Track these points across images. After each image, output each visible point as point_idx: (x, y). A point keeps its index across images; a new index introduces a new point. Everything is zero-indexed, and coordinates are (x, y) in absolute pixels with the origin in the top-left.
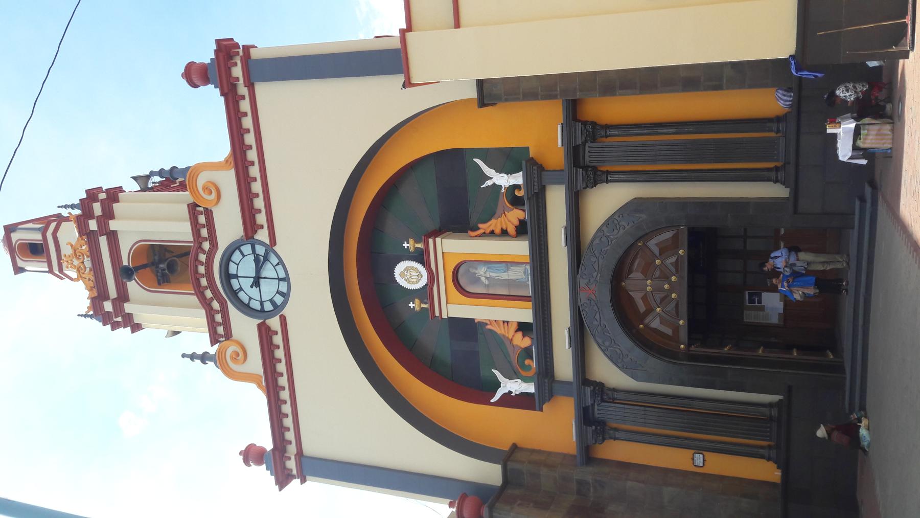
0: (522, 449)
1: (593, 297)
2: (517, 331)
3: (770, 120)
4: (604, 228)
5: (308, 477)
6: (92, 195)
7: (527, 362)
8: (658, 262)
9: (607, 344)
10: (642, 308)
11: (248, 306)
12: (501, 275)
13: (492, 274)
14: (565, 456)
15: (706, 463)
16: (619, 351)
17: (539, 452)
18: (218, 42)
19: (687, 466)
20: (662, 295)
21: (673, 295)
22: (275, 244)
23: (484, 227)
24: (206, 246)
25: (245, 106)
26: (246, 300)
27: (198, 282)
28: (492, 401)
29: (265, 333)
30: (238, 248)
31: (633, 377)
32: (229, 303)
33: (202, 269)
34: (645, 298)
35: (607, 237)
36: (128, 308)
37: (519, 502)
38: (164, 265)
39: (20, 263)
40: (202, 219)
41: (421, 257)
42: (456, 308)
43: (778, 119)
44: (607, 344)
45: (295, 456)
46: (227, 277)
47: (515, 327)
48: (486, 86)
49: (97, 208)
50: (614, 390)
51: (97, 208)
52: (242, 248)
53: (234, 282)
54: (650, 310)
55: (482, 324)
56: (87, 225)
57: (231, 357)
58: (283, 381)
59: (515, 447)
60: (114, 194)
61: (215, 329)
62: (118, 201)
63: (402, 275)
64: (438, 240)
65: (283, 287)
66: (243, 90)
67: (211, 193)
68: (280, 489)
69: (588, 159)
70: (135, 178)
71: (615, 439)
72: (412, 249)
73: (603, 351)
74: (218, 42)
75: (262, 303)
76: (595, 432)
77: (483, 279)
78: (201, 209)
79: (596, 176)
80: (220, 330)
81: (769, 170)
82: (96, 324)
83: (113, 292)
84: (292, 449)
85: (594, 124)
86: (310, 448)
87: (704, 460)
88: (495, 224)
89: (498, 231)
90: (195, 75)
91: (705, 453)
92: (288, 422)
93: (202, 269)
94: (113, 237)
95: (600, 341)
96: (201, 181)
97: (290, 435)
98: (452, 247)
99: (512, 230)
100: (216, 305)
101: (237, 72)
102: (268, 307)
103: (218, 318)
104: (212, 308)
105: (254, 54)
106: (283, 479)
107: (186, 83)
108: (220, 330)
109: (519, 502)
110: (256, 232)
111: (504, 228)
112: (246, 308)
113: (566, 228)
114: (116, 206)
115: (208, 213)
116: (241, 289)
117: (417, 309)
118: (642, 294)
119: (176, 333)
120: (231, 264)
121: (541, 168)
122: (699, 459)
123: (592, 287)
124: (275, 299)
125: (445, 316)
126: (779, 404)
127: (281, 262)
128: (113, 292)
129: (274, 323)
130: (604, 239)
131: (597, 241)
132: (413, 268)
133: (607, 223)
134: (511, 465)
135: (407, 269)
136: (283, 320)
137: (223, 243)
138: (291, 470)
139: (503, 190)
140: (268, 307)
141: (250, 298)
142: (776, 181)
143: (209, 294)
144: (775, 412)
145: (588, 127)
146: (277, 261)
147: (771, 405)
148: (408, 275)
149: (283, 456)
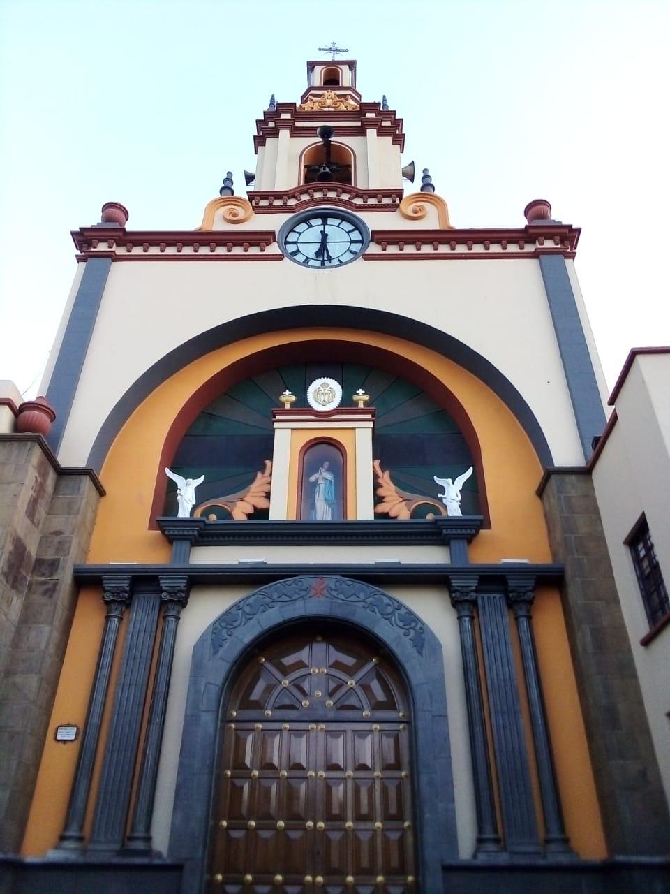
0: (98, 502)
1: (313, 592)
2: (254, 506)
3: (562, 828)
4: (403, 611)
5: (83, 264)
6: (398, 123)
7: (213, 518)
8: (351, 682)
9: (247, 609)
10: (288, 660)
11: (292, 231)
12: (321, 497)
13: (322, 487)
14: (85, 552)
15: (61, 744)
16: (238, 623)
17: (93, 523)
18: (579, 230)
19: (57, 717)
20: (306, 689)
21: (306, 703)
22: (365, 259)
23: (385, 477)
24: (358, 201)
25: (513, 248)
26: (295, 229)
27: (320, 190)
28: (167, 471)
29: (264, 238)
30: (357, 228)
31: (202, 640)
32: (293, 215)
33: (332, 195)
34: (300, 665)
35: (393, 613)
36: (285, 133)
37: (39, 479)
38: (328, 169)
39: (318, 69)
40: (386, 201)
41: (347, 405)
42: (287, 441)
43: (566, 841)
44: (247, 609)
45: (114, 252)
46: (324, 217)
47: (262, 504)
48: (573, 478)
49: (386, 123)
50: (178, 618)
51: (386, 123)
52: (357, 231)
53: (319, 221)
54: (285, 671)
55: (262, 468)
56: (371, 111)
57: (233, 209)
58: (204, 251)
59: (101, 493)
60: (399, 140)
61: (267, 199)
62: (394, 142)
63: (325, 386)
64: (371, 424)
65: (311, 263)
66: (529, 248)
67: (416, 212)
68: (73, 234)
69: (486, 596)
70: (413, 162)
71: (108, 618)
72: (355, 397)
73: (236, 606)
74: (579, 230)
75: (296, 243)
76: (118, 591)
77: (317, 475)
78: (398, 202)
79: (463, 605)
81: (496, 831)
82: (266, 106)
83: (298, 124)
84: (121, 251)
85: (531, 602)
86: (118, 269)
87: (64, 741)
88: (389, 489)
89: (381, 492)
90: (537, 209)
91: (77, 743)
94: (361, 132)
95: (251, 601)
96: (427, 206)
97: (137, 251)
98: (359, 440)
99: (383, 508)
101: (549, 244)
102: (291, 248)
104: (289, 198)
105: (568, 262)
106: (84, 238)
107: (528, 203)
108: (264, 203)
109: (39, 479)
110: (379, 243)
111: (385, 500)
112: (290, 228)
113: (399, 563)
114: (389, 139)
115: (394, 207)
116: (310, 226)
117: (283, 398)
118: (307, 662)
119: (249, 178)
120: (340, 221)
121: (470, 539)
122: (68, 734)
123: (325, 592)
124: (300, 255)
125: (276, 425)
126: (148, 852)
127: (341, 263)
128: (298, 124)
129: (273, 249)
130: (390, 609)
131: (386, 600)
132: (333, 396)
133: (410, 613)
134: (86, 482)
135: (332, 391)
136: (278, 258)
137: (362, 216)
138: (95, 247)
139: (440, 495)
140: (291, 248)
141: (300, 234)
142: (480, 841)
143: (305, 198)
144: (140, 845)
145: (530, 594)
146: (344, 259)
147: (148, 839)
148: (325, 392)
149: (115, 241)
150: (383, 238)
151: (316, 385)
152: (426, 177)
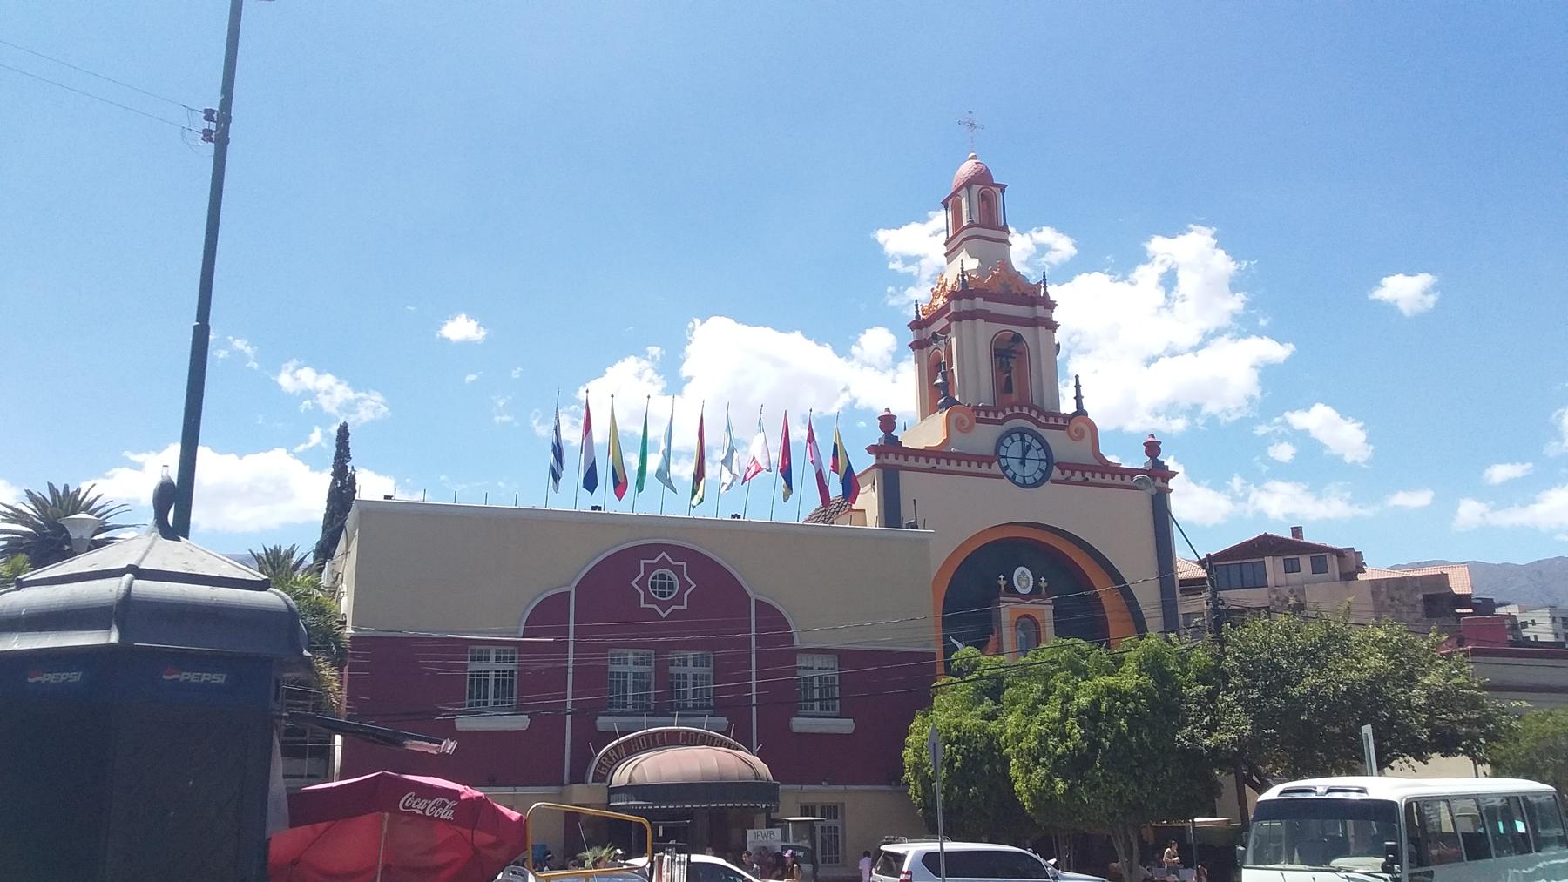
39: (976, 188)
40: (1060, 422)
41: (1036, 590)
53: (1017, 437)
65: (1018, 479)
80: (982, 415)
84: (901, 461)
90: (1153, 448)
92: (922, 463)
93: (1025, 411)
97: (911, 462)
100: (1001, 416)
103: (991, 416)
115: (1062, 428)
127: (1037, 484)
129: (996, 468)
136: (1000, 477)
137: (1043, 432)
148: (1023, 578)
150: (1063, 467)
151: (1018, 571)
152: (1078, 386)
